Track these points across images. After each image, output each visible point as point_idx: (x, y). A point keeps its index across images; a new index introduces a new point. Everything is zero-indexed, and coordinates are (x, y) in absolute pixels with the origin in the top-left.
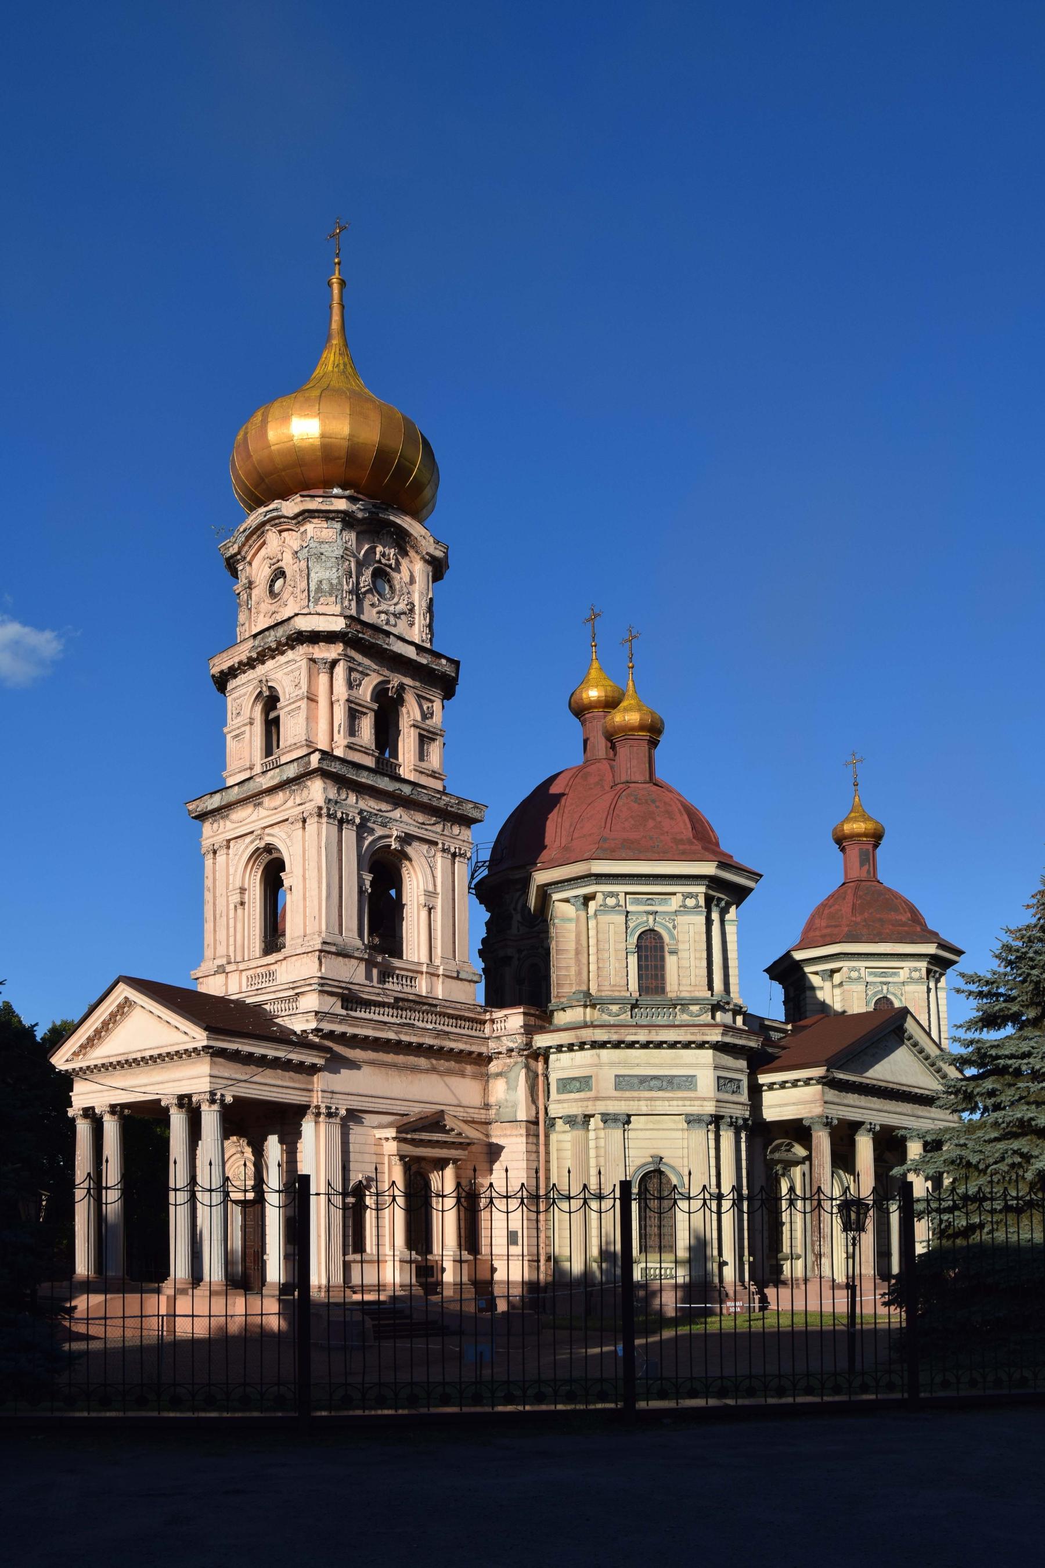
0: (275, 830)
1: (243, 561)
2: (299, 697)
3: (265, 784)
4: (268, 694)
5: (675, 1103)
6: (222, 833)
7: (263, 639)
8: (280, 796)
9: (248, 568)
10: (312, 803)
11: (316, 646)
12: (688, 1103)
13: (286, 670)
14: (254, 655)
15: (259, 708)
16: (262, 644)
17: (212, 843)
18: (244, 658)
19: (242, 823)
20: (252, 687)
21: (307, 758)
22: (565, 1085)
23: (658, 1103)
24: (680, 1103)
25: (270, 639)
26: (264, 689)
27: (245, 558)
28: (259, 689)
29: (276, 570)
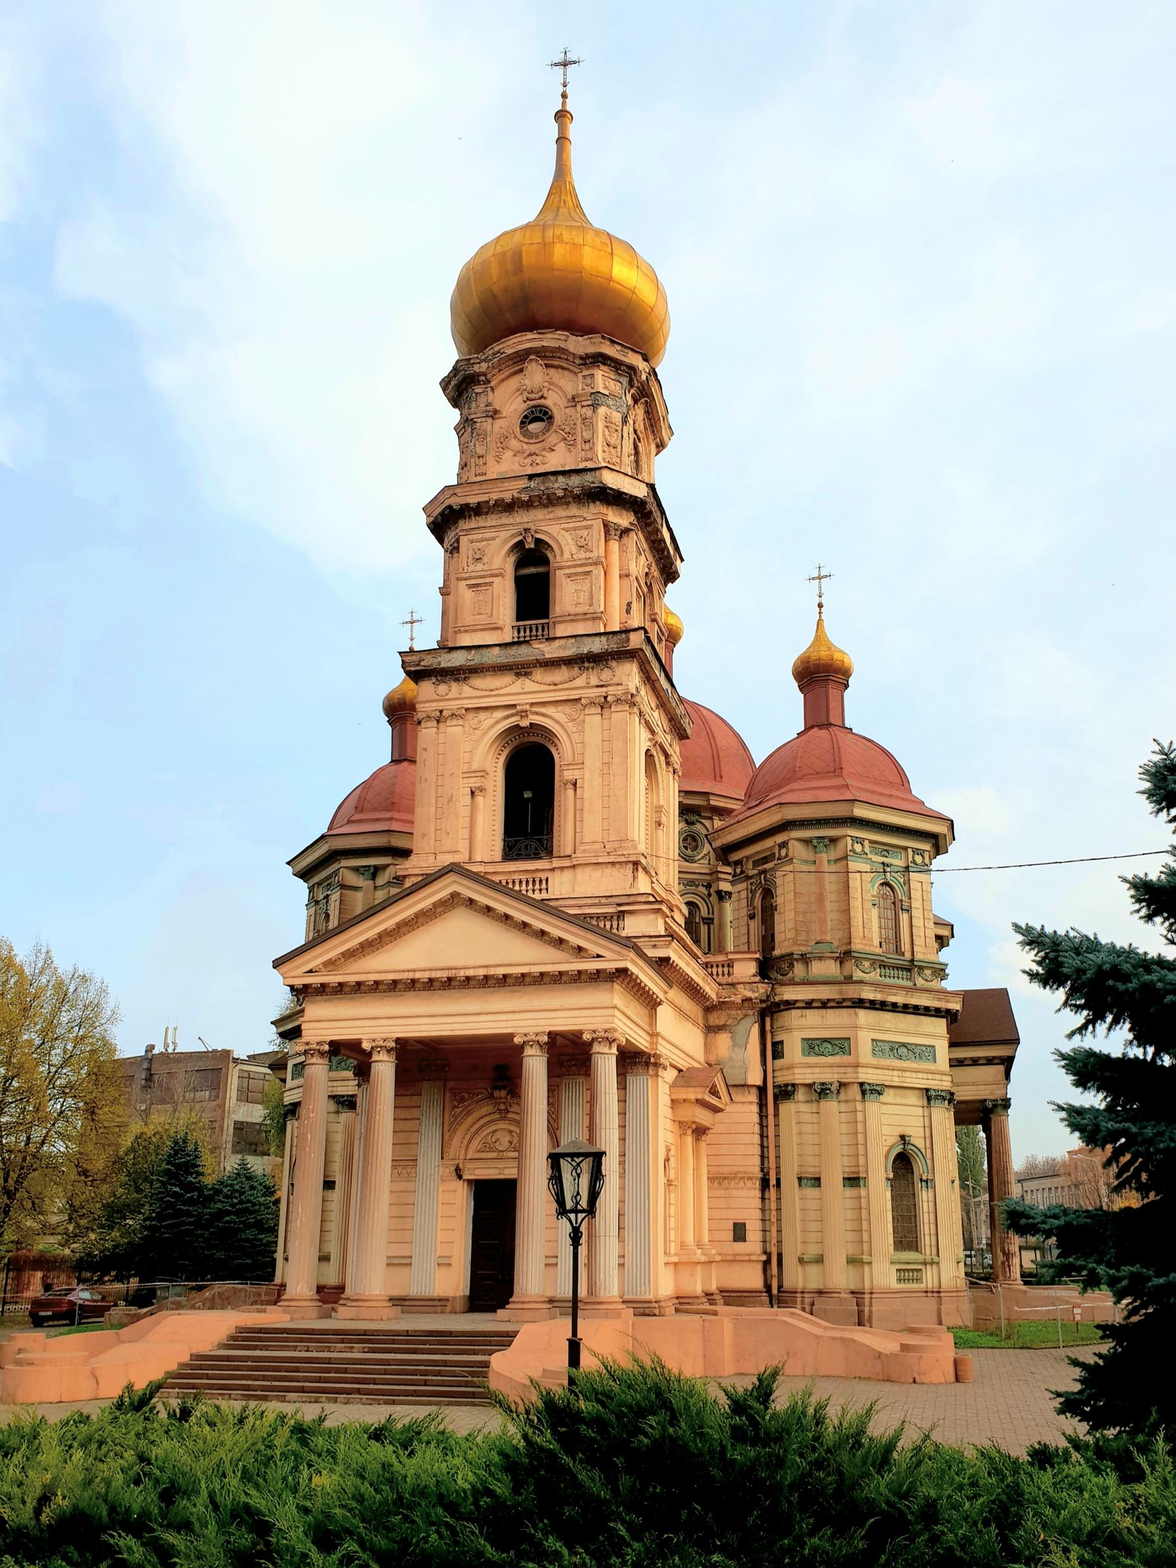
0: (549, 710)
1: (485, 384)
2: (590, 561)
3: (549, 653)
4: (532, 546)
5: (920, 1075)
6: (457, 699)
7: (543, 483)
8: (562, 674)
9: (490, 393)
10: (620, 688)
11: (610, 508)
12: (930, 1076)
13: (563, 526)
14: (525, 497)
15: (511, 561)
16: (542, 488)
17: (441, 708)
18: (507, 497)
19: (492, 693)
20: (509, 534)
21: (624, 636)
22: (813, 1046)
23: (907, 1074)
24: (925, 1076)
25: (556, 486)
26: (529, 539)
27: (489, 382)
28: (520, 538)
29: (535, 407)
